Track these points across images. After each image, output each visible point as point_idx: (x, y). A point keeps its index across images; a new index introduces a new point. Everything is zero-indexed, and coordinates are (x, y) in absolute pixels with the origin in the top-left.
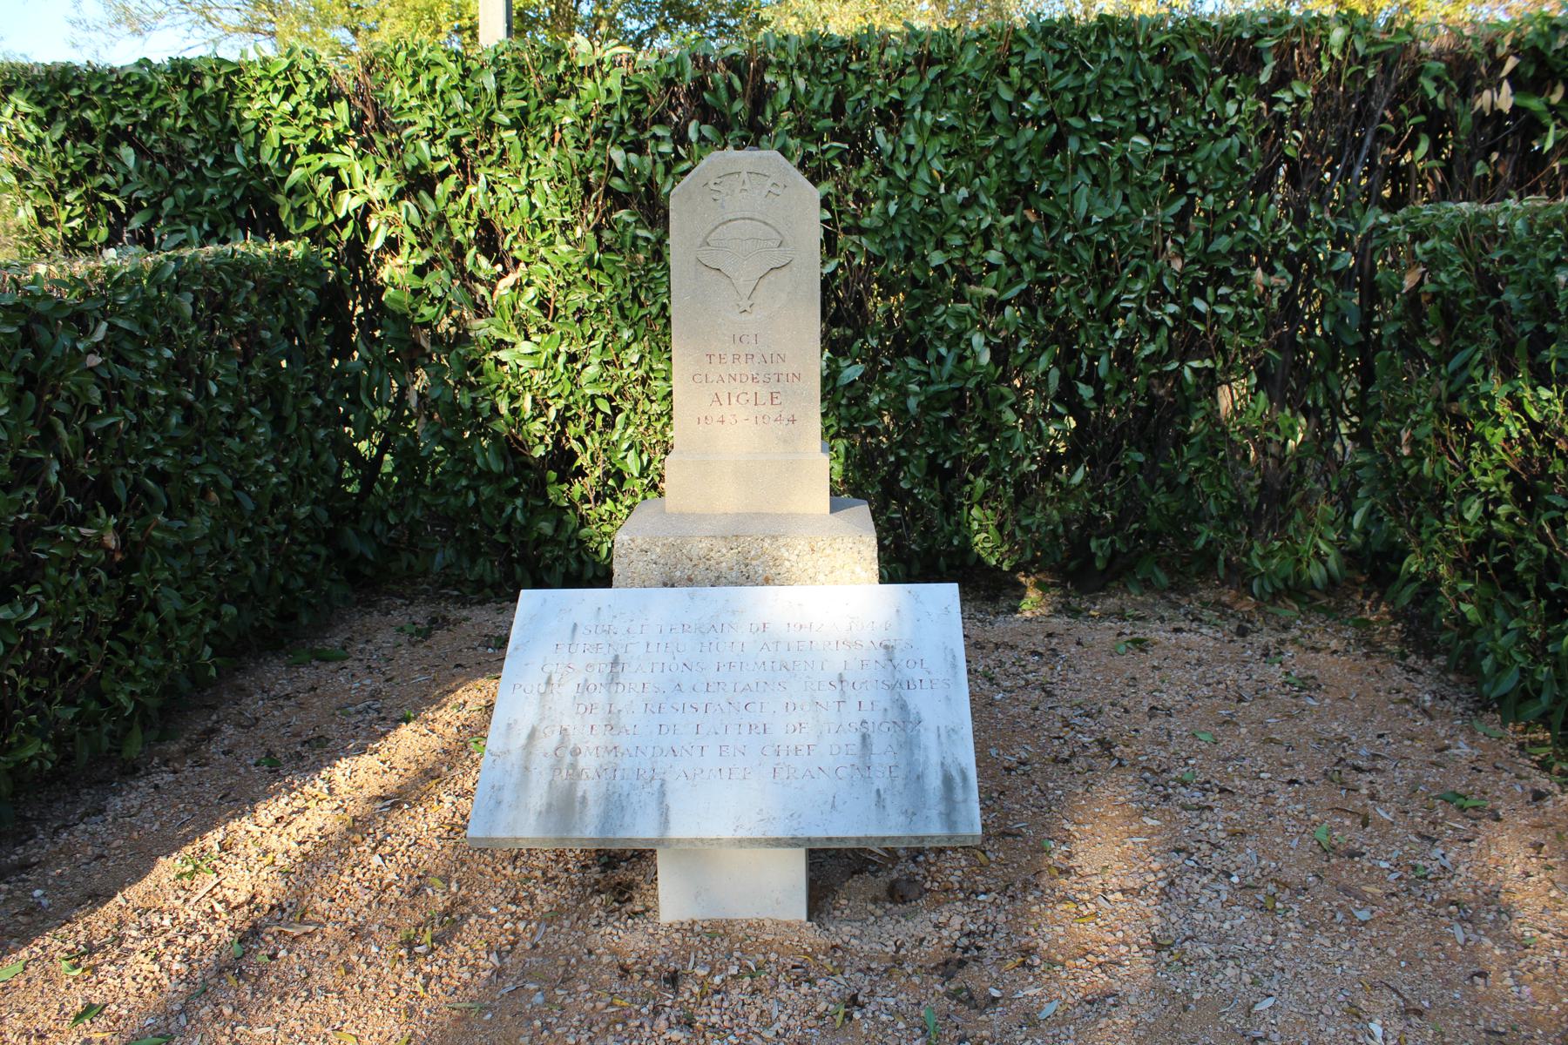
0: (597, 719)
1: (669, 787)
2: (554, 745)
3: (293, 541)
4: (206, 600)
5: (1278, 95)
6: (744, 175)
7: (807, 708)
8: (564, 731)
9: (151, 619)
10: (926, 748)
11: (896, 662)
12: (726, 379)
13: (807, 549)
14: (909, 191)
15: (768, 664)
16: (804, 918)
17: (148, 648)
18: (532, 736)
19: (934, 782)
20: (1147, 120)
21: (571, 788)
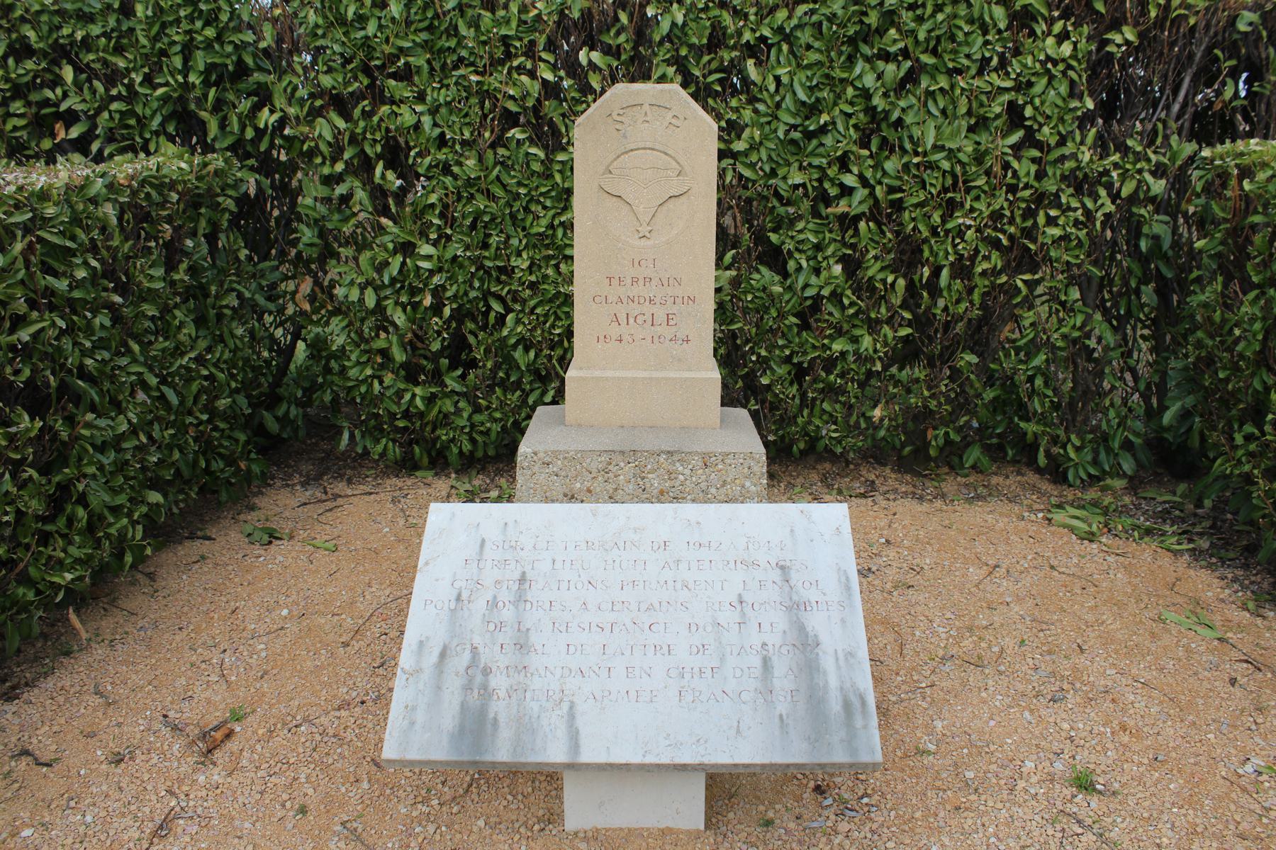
0: (506, 637)
1: (580, 708)
2: (465, 664)
3: (216, 428)
4: (132, 487)
5: (1109, 36)
6: (646, 107)
7: (709, 629)
8: (474, 649)
9: (81, 512)
10: (825, 673)
11: (792, 583)
12: (625, 300)
13: (700, 464)
14: (777, 118)
15: (670, 583)
16: (702, 827)
17: (77, 538)
18: (443, 655)
19: (835, 706)
20: (991, 58)
21: (482, 713)
